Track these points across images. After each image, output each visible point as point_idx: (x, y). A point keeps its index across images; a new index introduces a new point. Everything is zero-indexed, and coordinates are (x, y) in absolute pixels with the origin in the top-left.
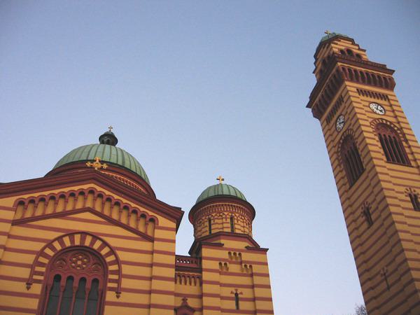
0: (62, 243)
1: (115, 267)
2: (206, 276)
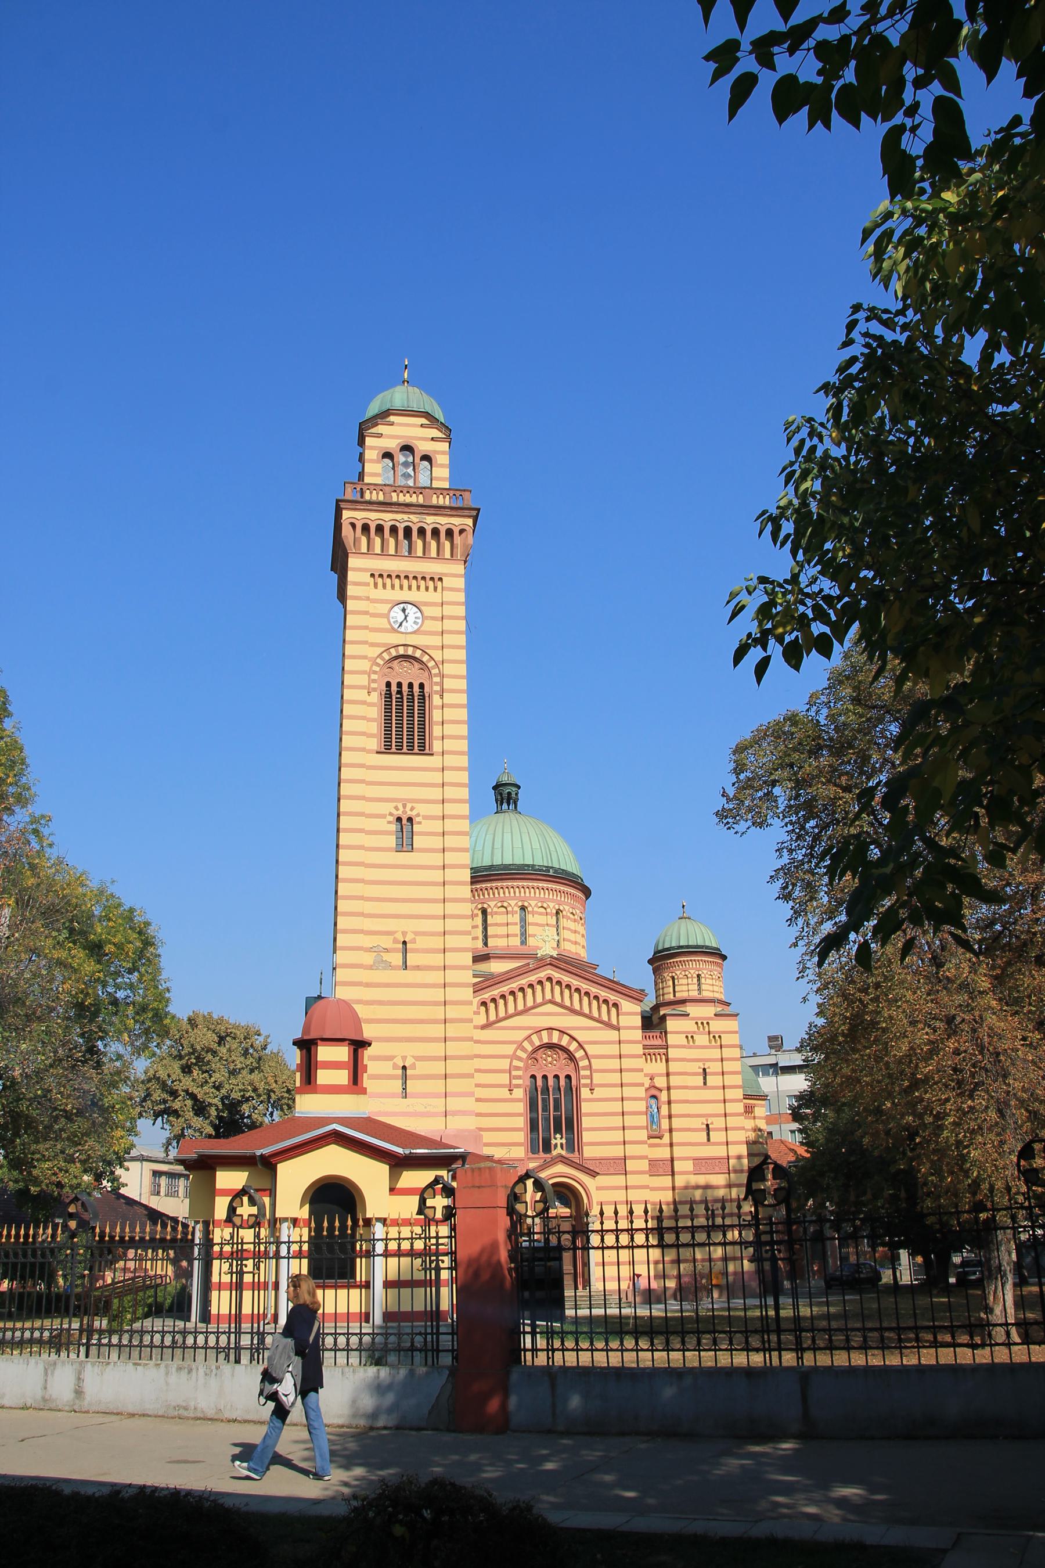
0: (532, 1043)
2: (672, 1053)
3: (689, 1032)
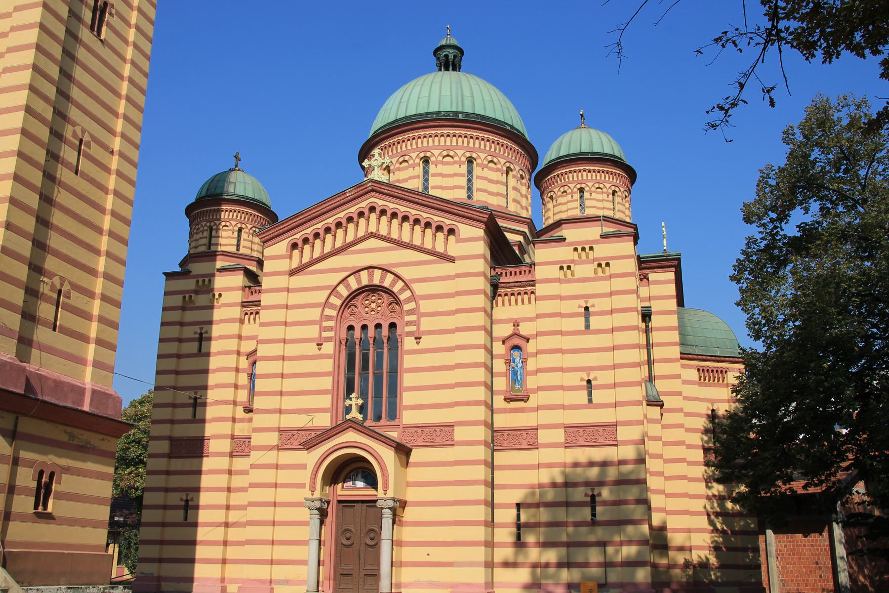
1: (411, 306)
2: (540, 289)
3: (564, 262)
